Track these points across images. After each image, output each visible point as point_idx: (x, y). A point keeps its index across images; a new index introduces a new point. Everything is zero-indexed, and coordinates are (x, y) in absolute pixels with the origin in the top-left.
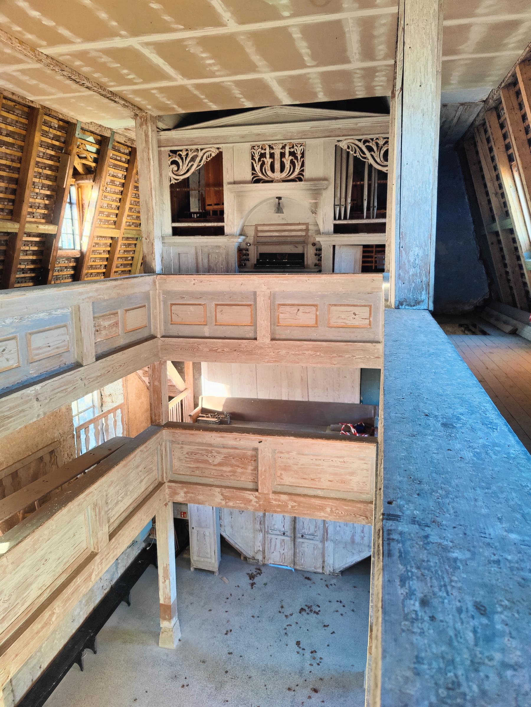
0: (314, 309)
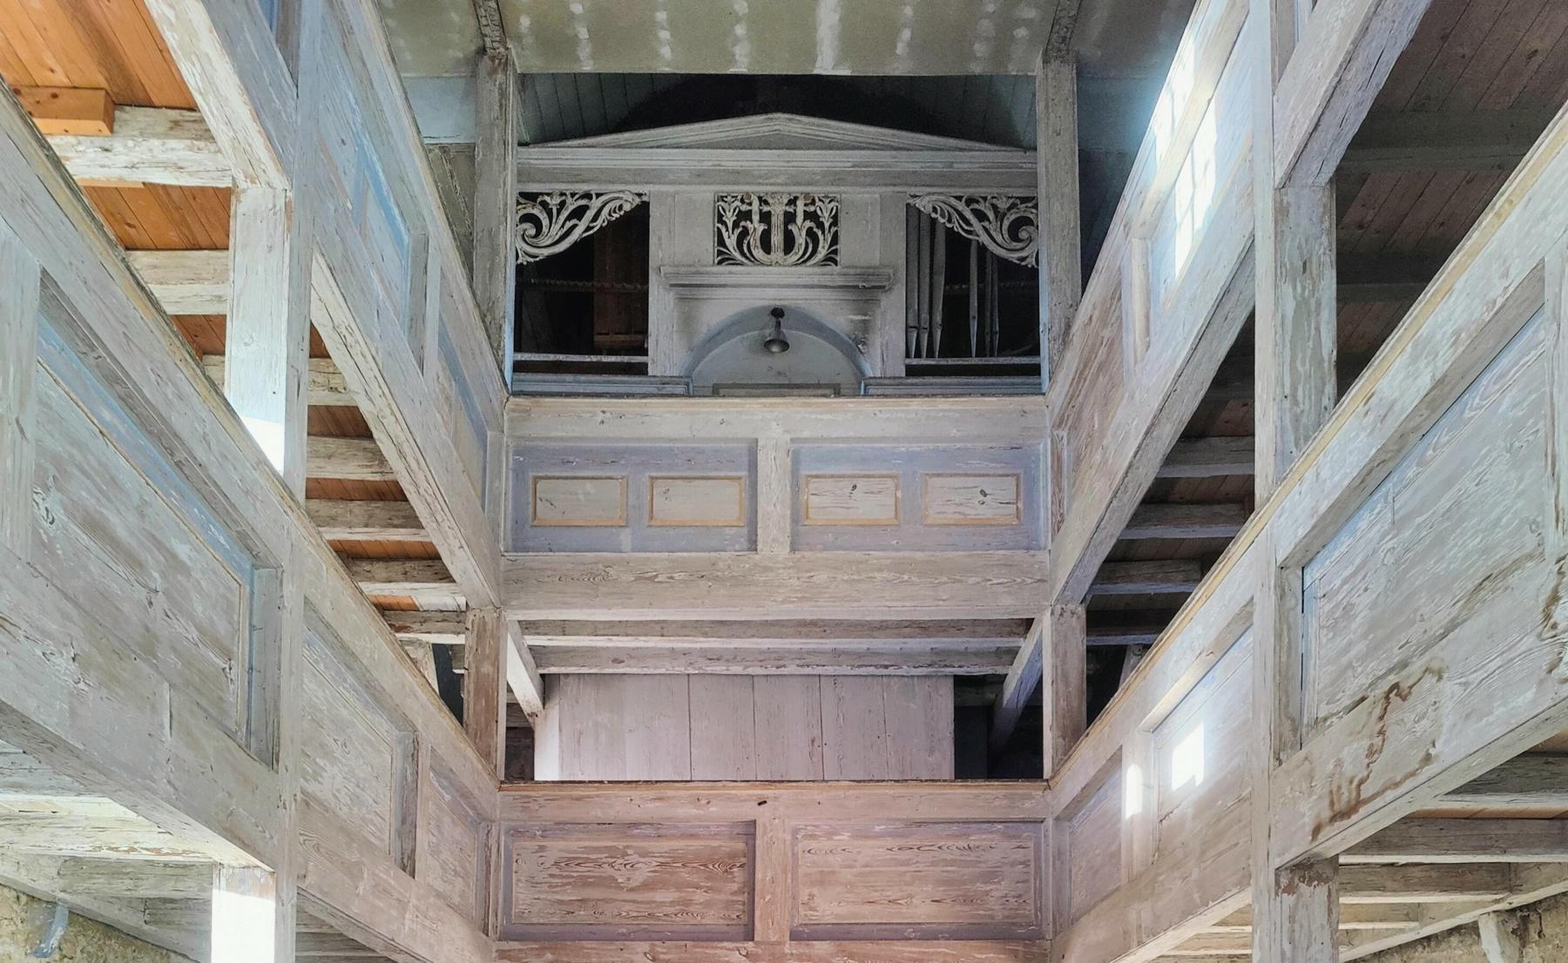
0: (890, 483)
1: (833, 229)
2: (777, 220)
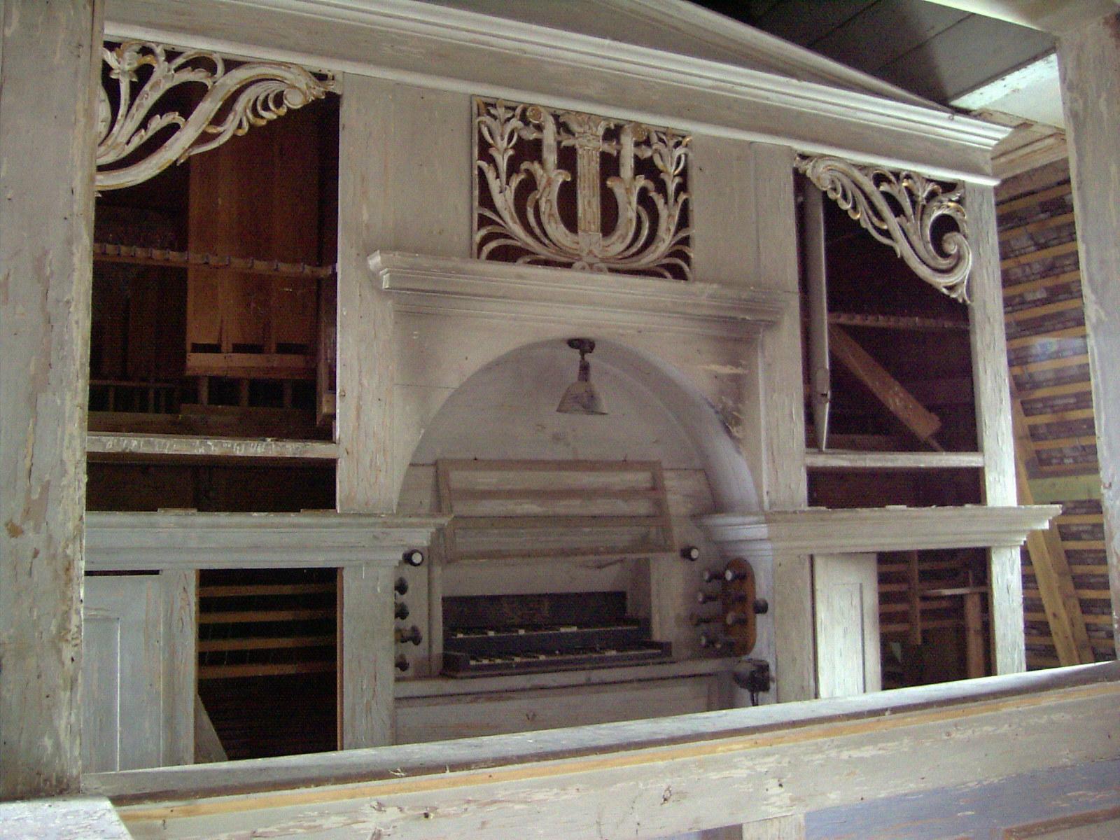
1: (683, 197)
2: (588, 166)
